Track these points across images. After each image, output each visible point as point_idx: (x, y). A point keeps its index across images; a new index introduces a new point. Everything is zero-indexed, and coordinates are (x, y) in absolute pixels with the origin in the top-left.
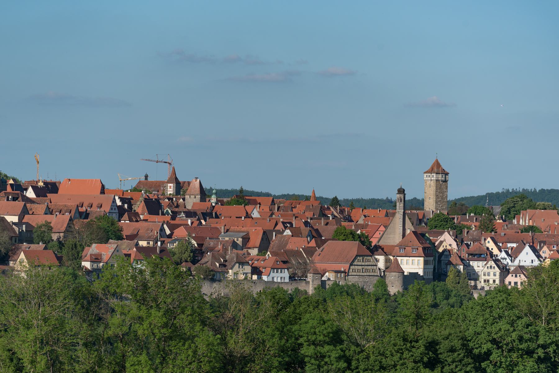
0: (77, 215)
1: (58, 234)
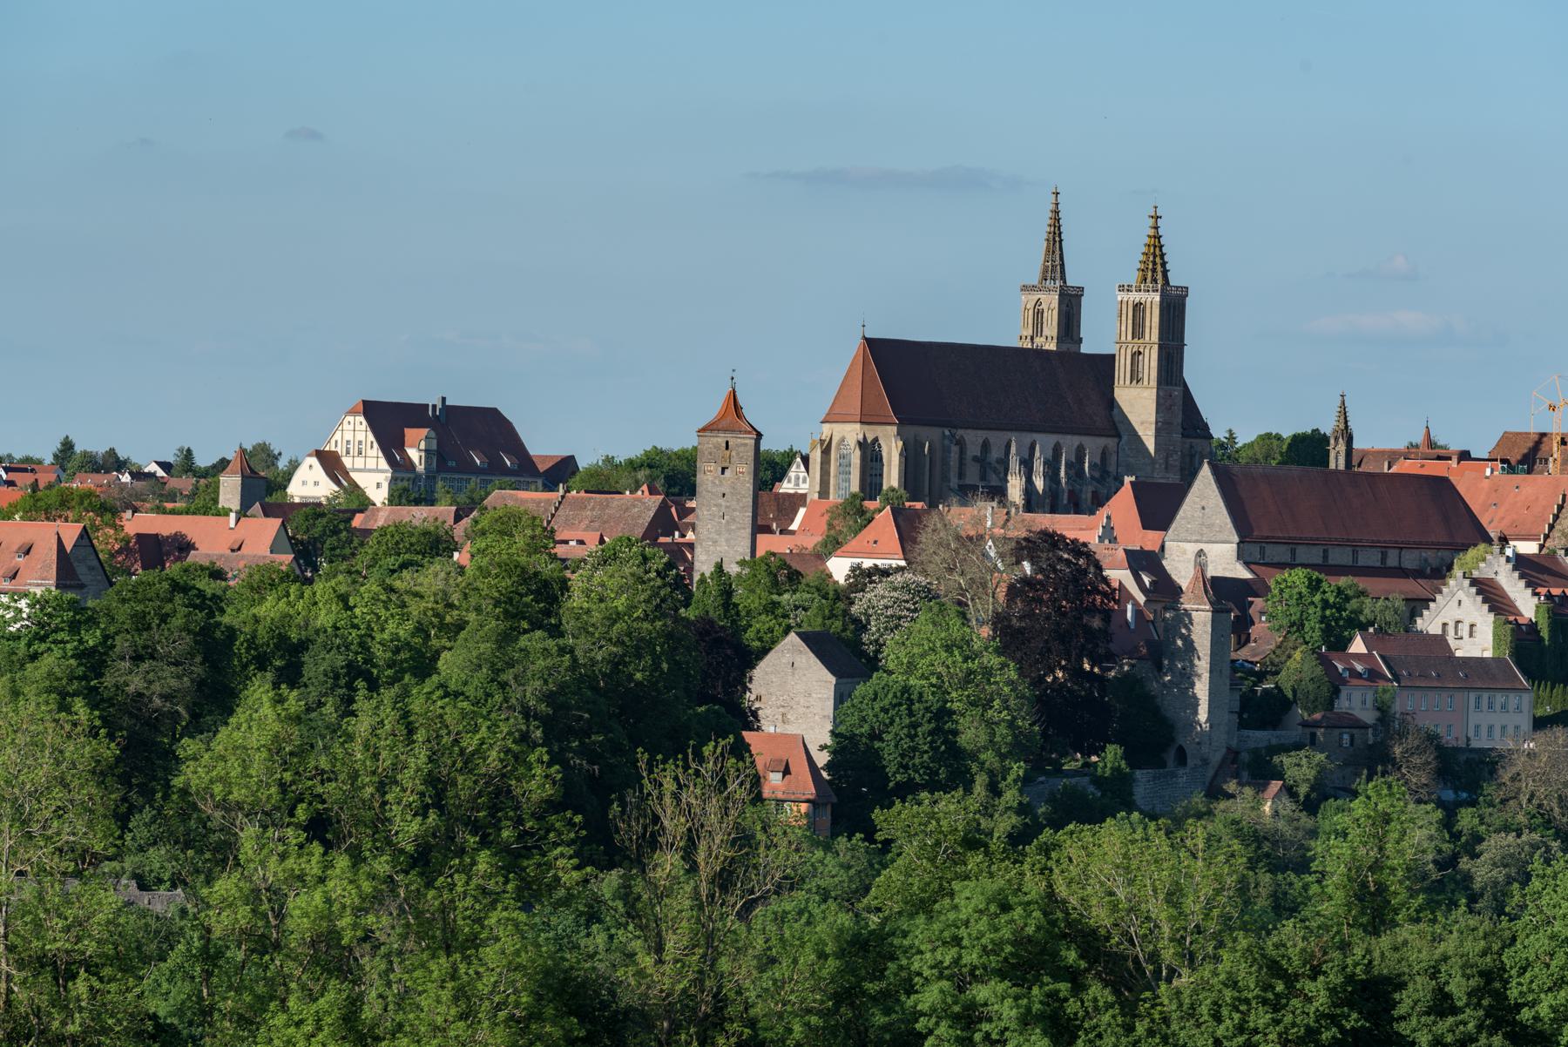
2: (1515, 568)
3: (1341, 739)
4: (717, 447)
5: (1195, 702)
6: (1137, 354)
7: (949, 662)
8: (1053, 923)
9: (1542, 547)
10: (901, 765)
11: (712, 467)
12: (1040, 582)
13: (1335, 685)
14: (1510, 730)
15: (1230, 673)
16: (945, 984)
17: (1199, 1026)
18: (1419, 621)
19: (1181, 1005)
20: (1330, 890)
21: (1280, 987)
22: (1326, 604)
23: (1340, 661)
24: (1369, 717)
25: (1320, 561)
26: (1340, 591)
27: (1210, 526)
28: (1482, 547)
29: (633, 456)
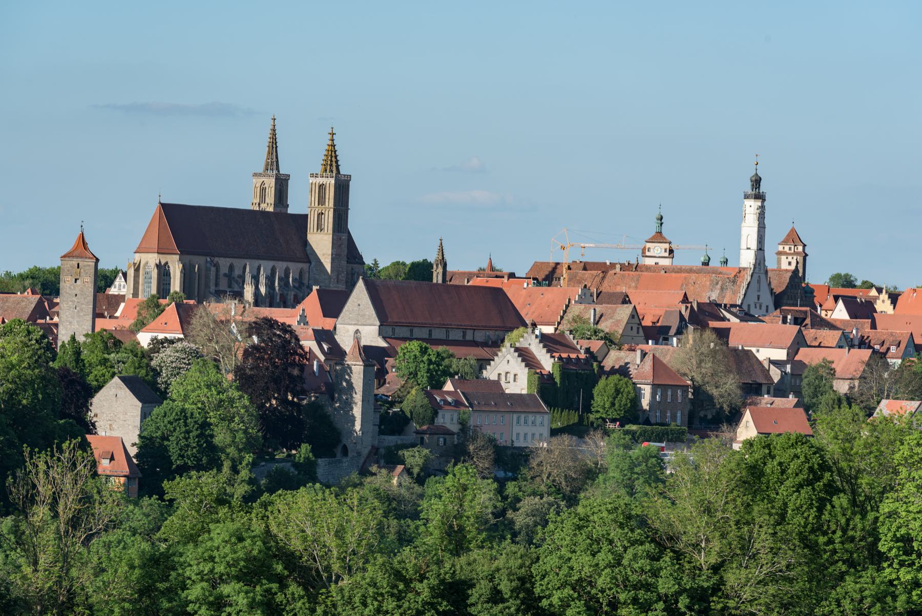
0: (912, 349)
1: (848, 382)
2: (541, 342)
3: (438, 441)
4: (72, 267)
5: (353, 419)
7: (209, 394)
8: (269, 549)
9: (556, 329)
10: (180, 455)
11: (69, 278)
12: (263, 348)
13: (435, 409)
14: (537, 436)
15: (374, 402)
16: (204, 584)
17: (353, 609)
18: (484, 372)
19: (343, 597)
20: (431, 529)
21: (401, 586)
22: (430, 362)
23: (438, 395)
24: (455, 428)
25: (427, 337)
26: (438, 354)
27: (363, 316)
28: (522, 329)
29: (22, 272)
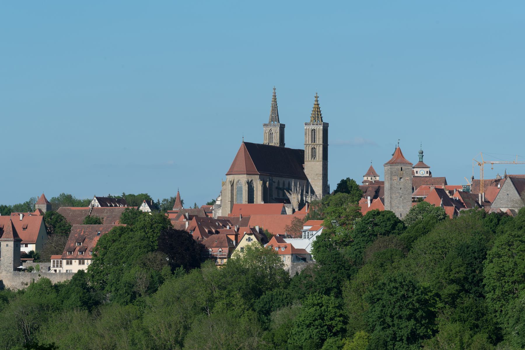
6: (313, 149)
